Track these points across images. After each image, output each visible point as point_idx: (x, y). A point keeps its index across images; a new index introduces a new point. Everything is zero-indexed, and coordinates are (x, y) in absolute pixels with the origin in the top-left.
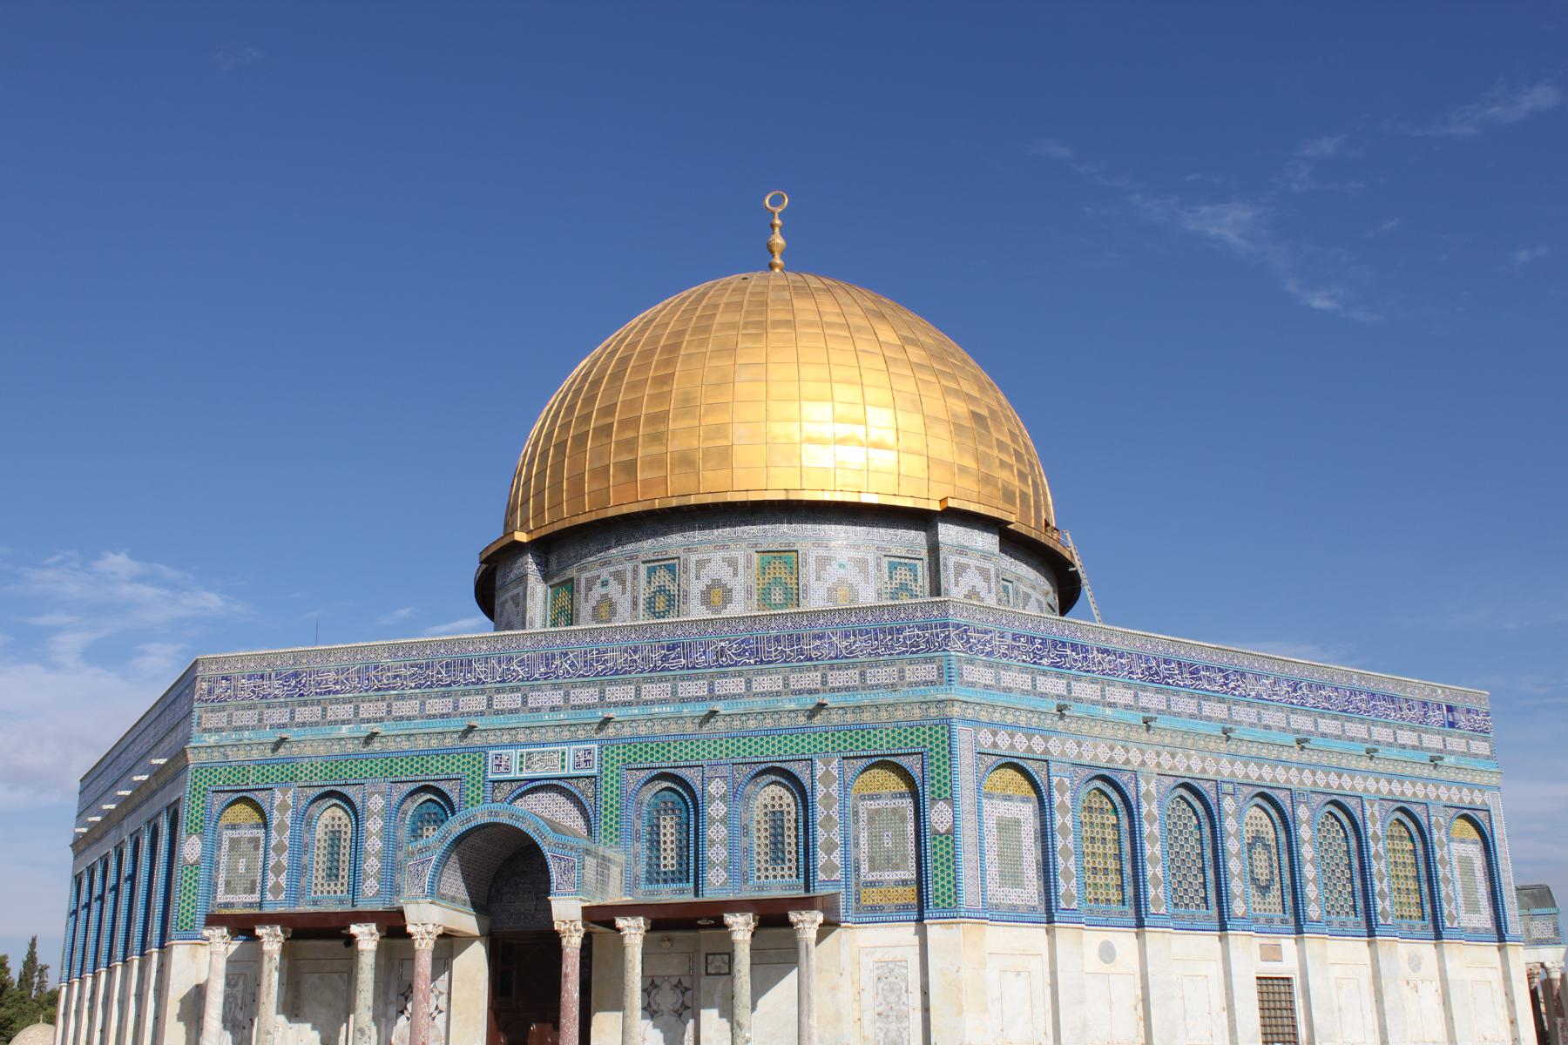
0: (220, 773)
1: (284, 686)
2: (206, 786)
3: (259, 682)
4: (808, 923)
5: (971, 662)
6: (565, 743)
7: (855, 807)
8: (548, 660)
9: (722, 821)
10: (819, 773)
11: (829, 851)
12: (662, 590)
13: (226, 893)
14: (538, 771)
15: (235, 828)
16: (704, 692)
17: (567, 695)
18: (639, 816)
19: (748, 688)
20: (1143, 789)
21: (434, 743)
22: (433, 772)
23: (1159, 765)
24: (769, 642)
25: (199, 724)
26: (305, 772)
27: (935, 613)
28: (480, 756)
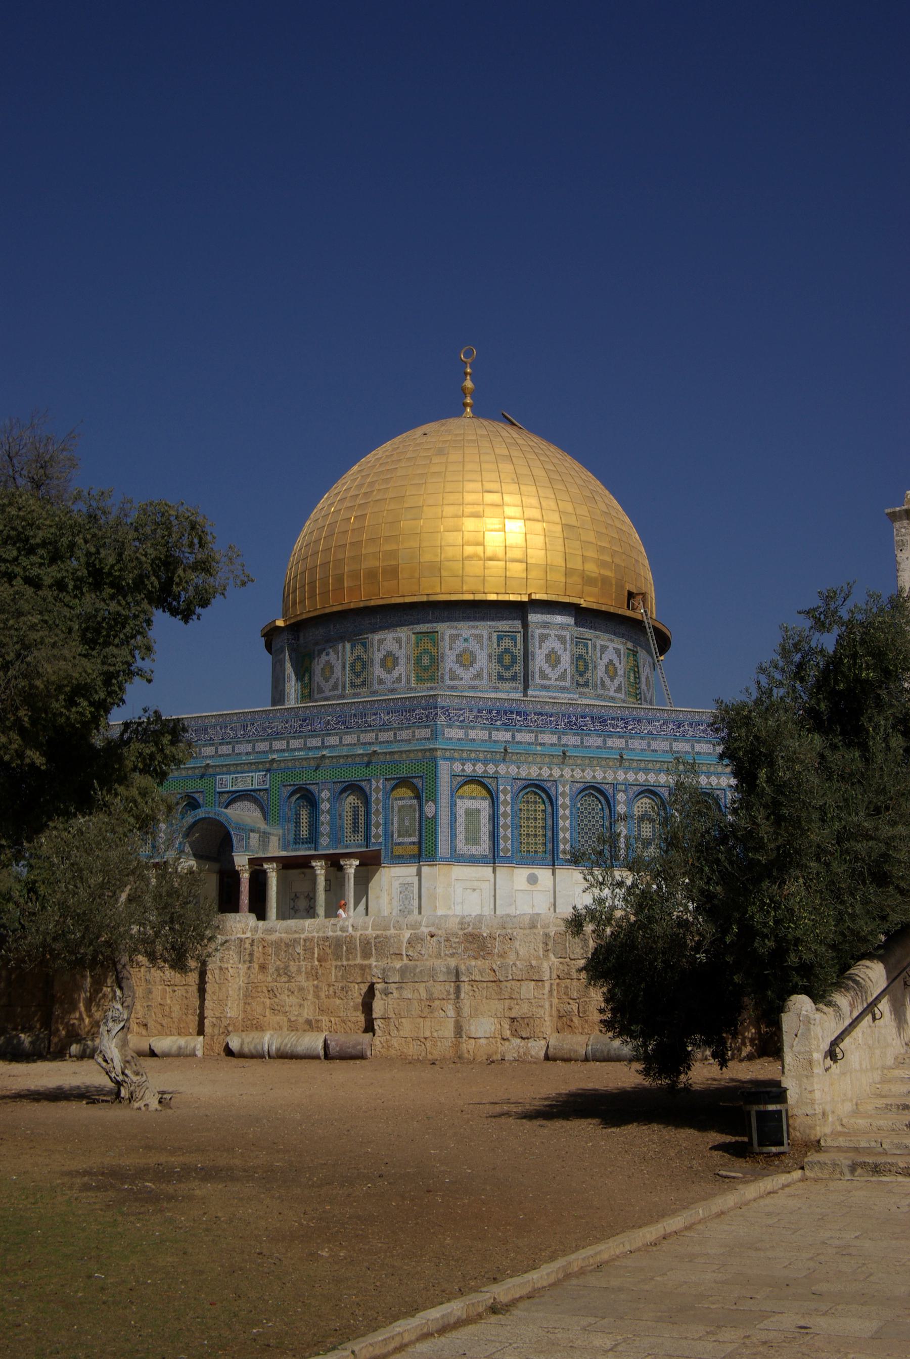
4: (351, 866)
5: (450, 726)
6: (253, 772)
7: (393, 804)
8: (245, 727)
9: (328, 812)
10: (373, 787)
12: (359, 658)
14: (241, 787)
16: (319, 744)
17: (254, 746)
18: (290, 810)
19: (341, 742)
20: (561, 789)
23: (572, 776)
24: (351, 717)
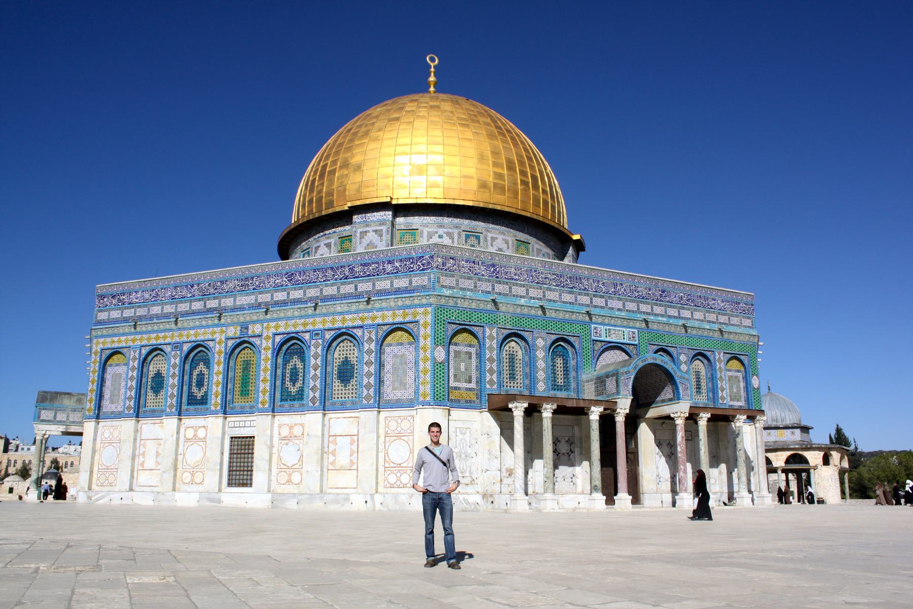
0: (453, 313)
1: (487, 270)
2: (445, 319)
3: (472, 265)
8: (615, 285)
11: (722, 391)
13: (455, 381)
14: (613, 338)
15: (456, 345)
19: (692, 316)
21: (567, 316)
22: (566, 331)
25: (439, 282)
26: (502, 320)
27: (749, 299)
28: (588, 327)
